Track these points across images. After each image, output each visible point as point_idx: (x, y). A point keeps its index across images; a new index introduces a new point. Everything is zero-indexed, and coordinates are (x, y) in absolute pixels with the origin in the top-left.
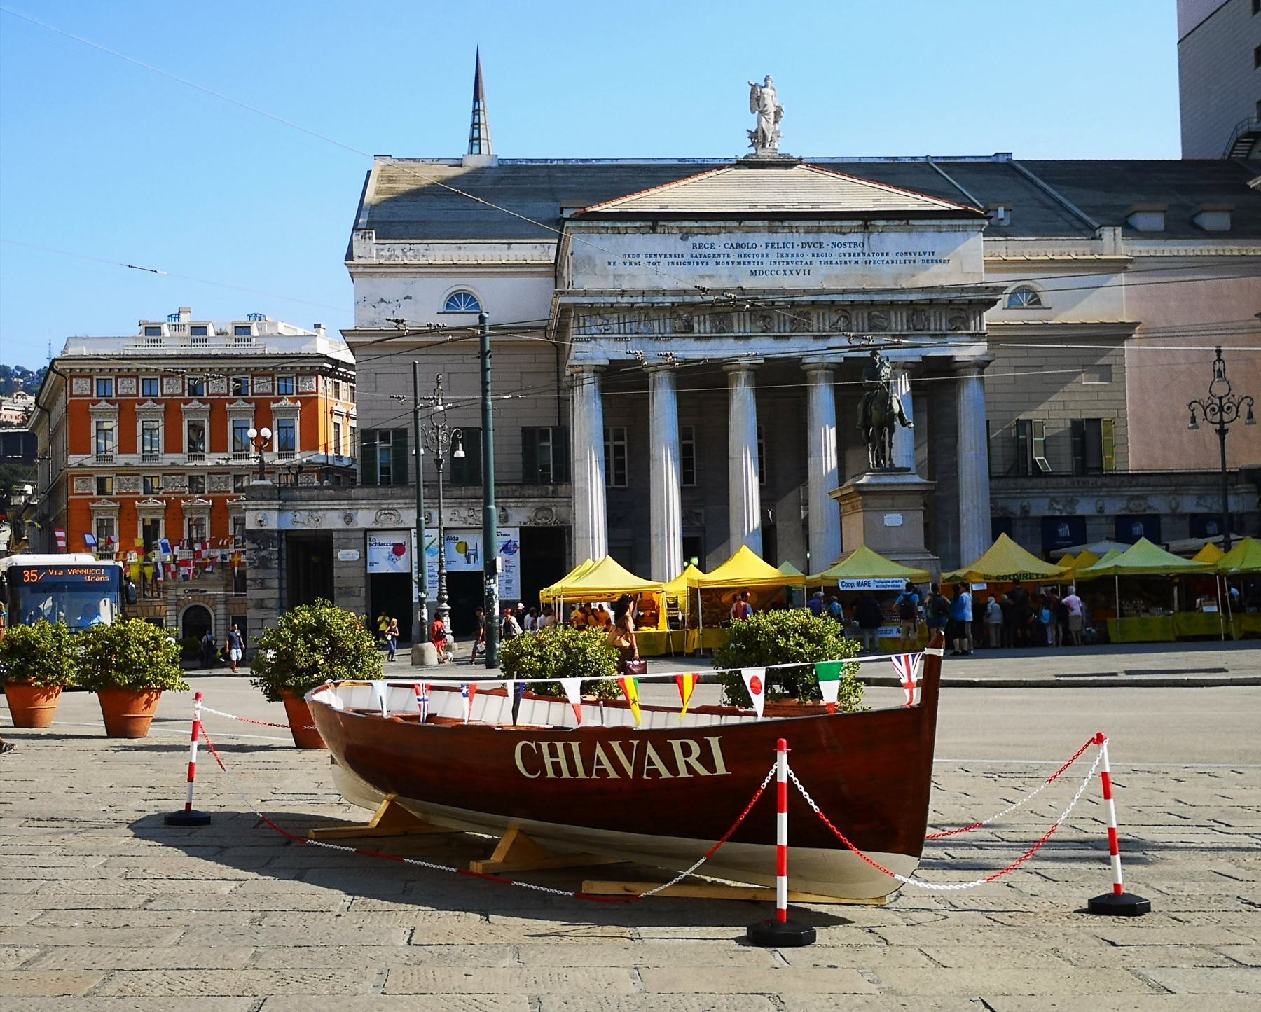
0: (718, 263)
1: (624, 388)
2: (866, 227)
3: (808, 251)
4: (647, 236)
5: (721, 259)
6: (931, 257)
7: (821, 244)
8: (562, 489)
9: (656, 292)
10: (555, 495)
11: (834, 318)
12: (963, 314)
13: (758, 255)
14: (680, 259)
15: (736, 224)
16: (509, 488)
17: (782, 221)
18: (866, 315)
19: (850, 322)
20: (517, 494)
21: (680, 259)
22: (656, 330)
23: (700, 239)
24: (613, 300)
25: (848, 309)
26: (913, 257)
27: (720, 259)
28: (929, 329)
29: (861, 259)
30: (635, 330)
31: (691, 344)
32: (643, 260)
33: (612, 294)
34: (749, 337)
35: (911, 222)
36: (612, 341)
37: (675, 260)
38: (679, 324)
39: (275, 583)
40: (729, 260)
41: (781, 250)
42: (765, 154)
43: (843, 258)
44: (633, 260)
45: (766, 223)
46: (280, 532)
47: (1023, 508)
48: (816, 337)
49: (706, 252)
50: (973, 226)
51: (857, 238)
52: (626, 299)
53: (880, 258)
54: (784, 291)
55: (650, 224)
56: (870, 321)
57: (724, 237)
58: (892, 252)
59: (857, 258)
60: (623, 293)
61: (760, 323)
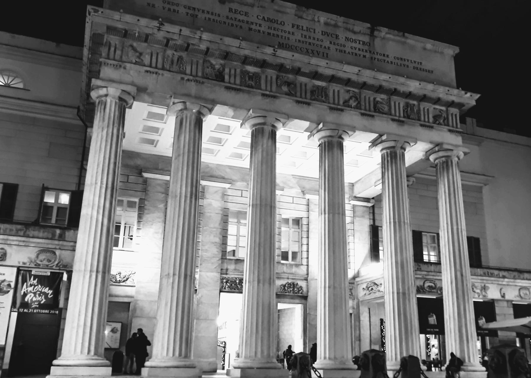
0: (250, 29)
2: (372, 30)
5: (253, 27)
6: (419, 66)
7: (337, 37)
8: (69, 234)
10: (62, 237)
18: (372, 99)
21: (216, 18)
22: (188, 71)
32: (182, 10)
35: (406, 34)
37: (212, 17)
40: (262, 29)
41: (305, 33)
43: (354, 51)
44: (172, 8)
49: (242, 18)
58: (392, 56)
59: (365, 54)
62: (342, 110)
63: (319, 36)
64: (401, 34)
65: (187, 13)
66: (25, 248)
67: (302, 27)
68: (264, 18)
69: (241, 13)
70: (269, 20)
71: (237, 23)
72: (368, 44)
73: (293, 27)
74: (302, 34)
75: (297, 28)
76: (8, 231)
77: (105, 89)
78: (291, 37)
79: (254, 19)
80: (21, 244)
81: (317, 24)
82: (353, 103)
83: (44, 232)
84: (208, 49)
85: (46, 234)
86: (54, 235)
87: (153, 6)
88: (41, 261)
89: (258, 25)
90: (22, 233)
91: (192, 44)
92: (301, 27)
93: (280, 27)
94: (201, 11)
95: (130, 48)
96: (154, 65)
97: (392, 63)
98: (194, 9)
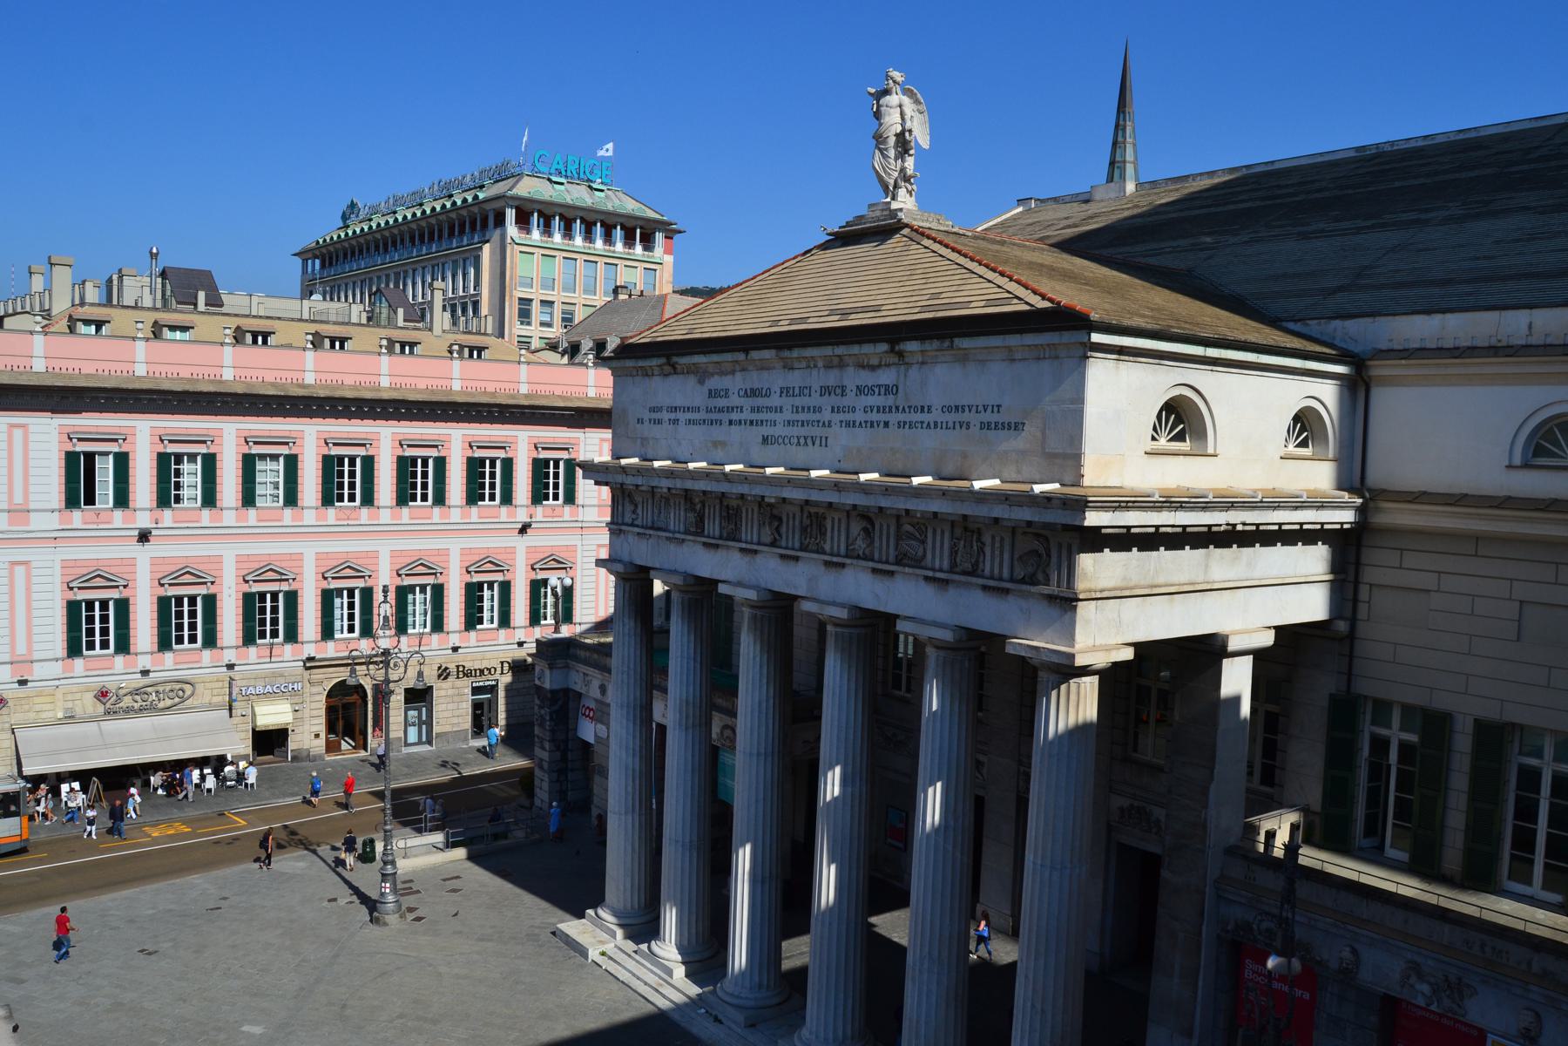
3: (826, 402)
5: (735, 416)
12: (1042, 550)
13: (769, 409)
15: (741, 356)
19: (872, 542)
26: (966, 417)
27: (735, 416)
29: (893, 418)
32: (666, 416)
35: (956, 341)
38: (692, 517)
39: (547, 745)
40: (743, 416)
41: (798, 401)
46: (552, 692)
51: (886, 377)
53: (918, 417)
63: (815, 400)
64: (947, 343)
70: (753, 393)
78: (778, 417)
81: (815, 372)
82: (860, 544)
97: (936, 424)
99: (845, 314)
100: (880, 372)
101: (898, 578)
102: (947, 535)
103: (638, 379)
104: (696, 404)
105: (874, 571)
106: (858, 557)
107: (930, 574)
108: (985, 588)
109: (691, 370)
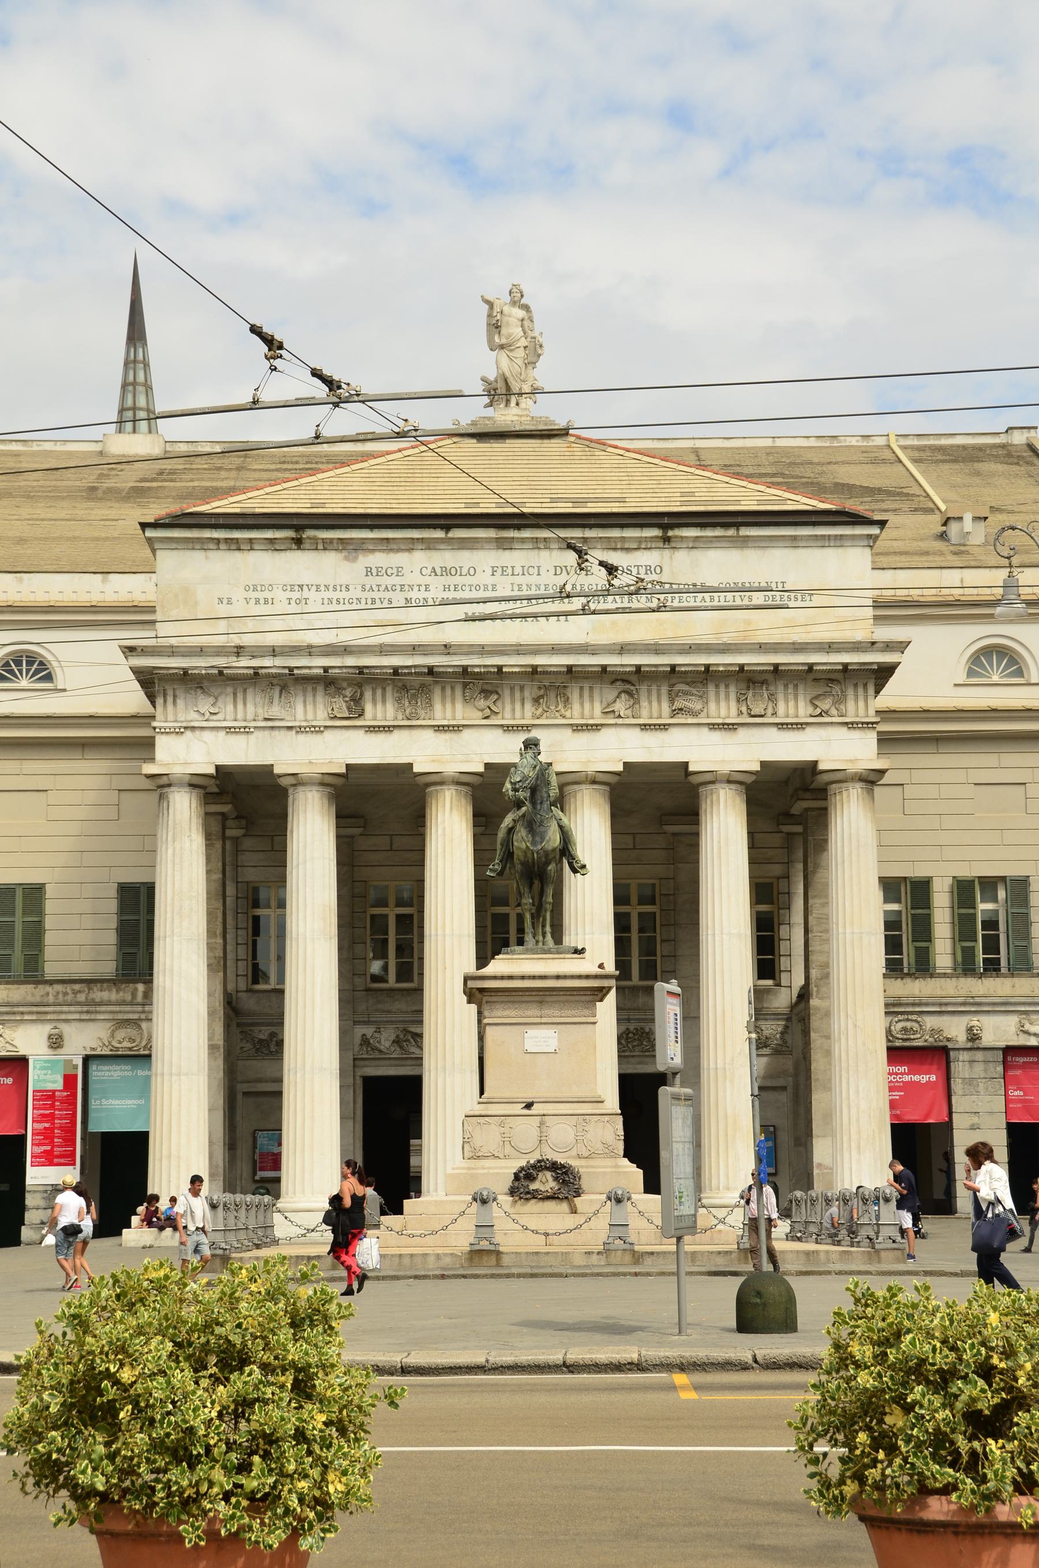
1: (245, 810)
2: (667, 540)
4: (289, 555)
5: (414, 595)
9: (295, 650)
11: (610, 693)
14: (344, 594)
16: (69, 988)
17: (518, 527)
18: (664, 690)
19: (637, 702)
20: (82, 998)
23: (378, 559)
24: (221, 661)
25: (634, 678)
28: (774, 714)
30: (262, 713)
31: (359, 737)
32: (279, 595)
33: (220, 651)
34: (457, 728)
35: (744, 531)
36: (222, 734)
42: (507, 416)
44: (261, 595)
45: (491, 533)
47: (970, 1030)
48: (578, 728)
50: (853, 537)
52: (245, 662)
54: (519, 650)
55: (290, 533)
56: (672, 701)
57: (420, 558)
60: (239, 651)
61: (482, 703)
62: (597, 727)
64: (731, 532)
65: (290, 599)
66: (91, 1024)
67: (513, 567)
68: (434, 570)
69: (389, 571)
70: (446, 571)
71: (381, 595)
72: (658, 571)
73: (493, 571)
74: (512, 584)
75: (502, 574)
76: (60, 996)
77: (165, 777)
79: (415, 578)
80: (84, 1016)
81: (544, 554)
82: (620, 706)
83: (118, 991)
84: (326, 669)
85: (121, 994)
86: (134, 995)
87: (229, 602)
88: (120, 1043)
89: (423, 588)
90: (82, 998)
91: (297, 668)
92: (510, 571)
93: (468, 580)
94: (314, 588)
95: (199, 691)
96: (240, 716)
98: (301, 587)
99: (575, 502)
100: (638, 554)
101: (673, 731)
102: (732, 689)
103: (211, 554)
104: (343, 579)
105: (644, 727)
106: (620, 716)
107: (720, 721)
108: (782, 726)
109: (327, 545)
